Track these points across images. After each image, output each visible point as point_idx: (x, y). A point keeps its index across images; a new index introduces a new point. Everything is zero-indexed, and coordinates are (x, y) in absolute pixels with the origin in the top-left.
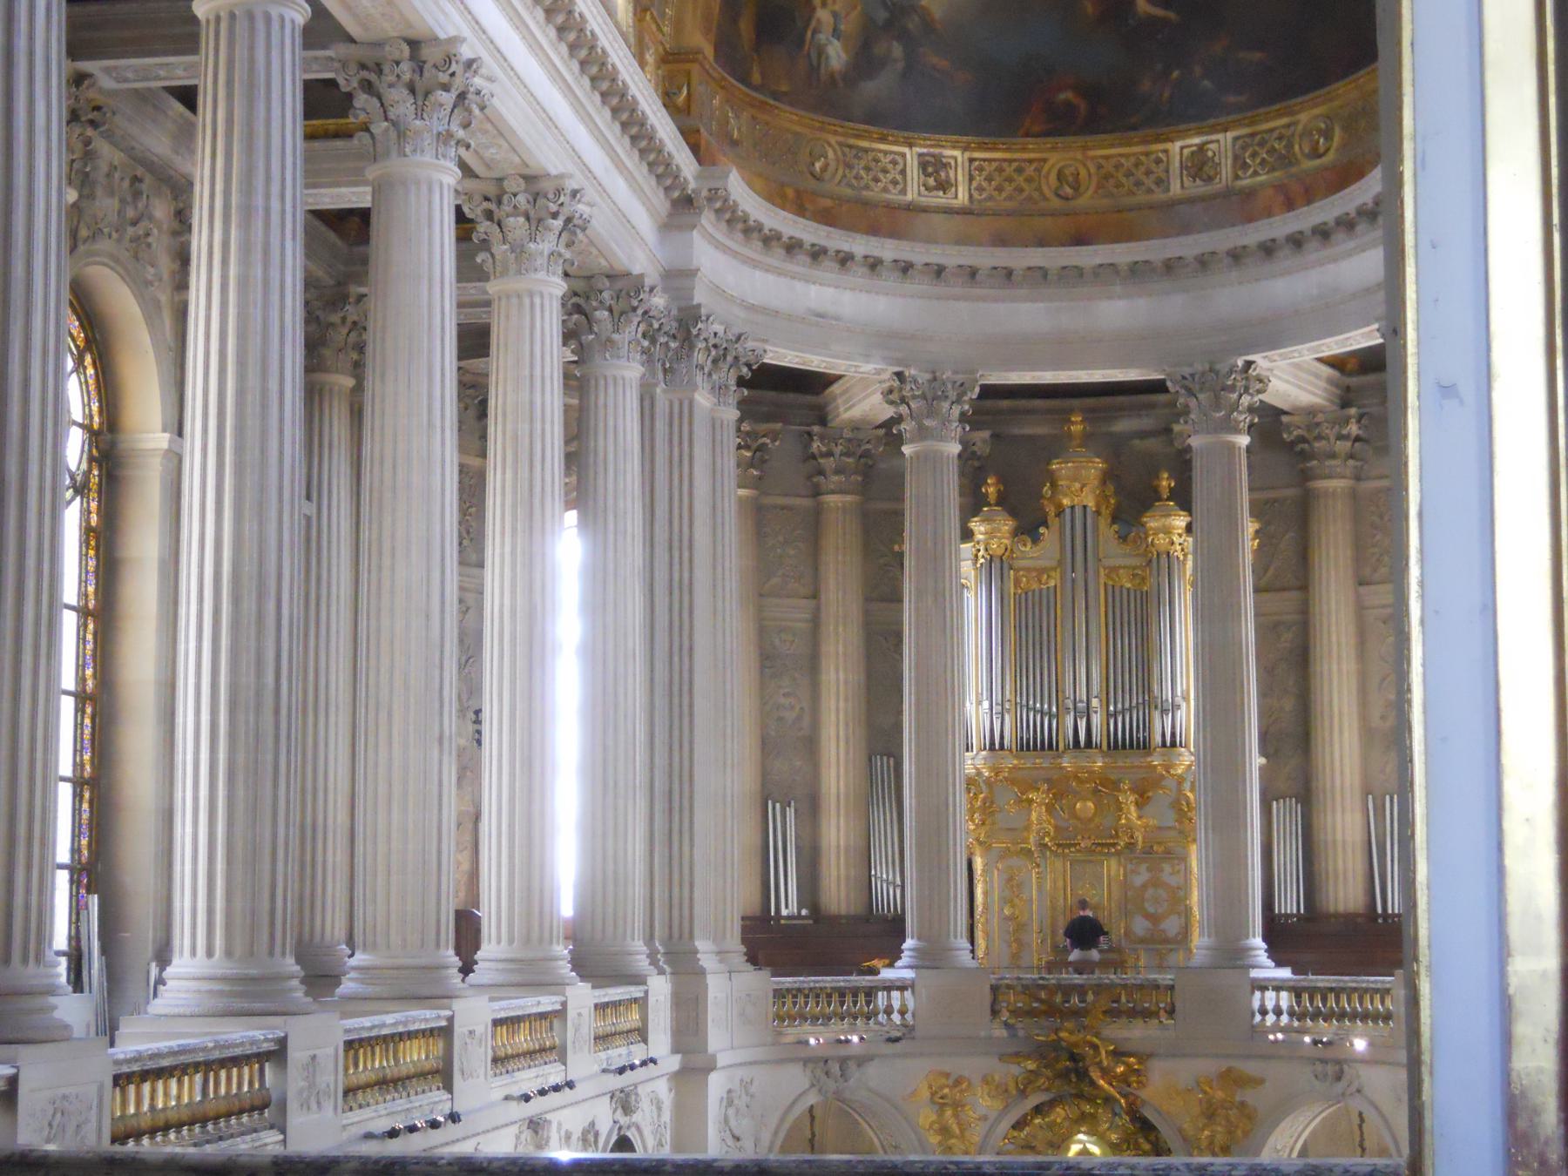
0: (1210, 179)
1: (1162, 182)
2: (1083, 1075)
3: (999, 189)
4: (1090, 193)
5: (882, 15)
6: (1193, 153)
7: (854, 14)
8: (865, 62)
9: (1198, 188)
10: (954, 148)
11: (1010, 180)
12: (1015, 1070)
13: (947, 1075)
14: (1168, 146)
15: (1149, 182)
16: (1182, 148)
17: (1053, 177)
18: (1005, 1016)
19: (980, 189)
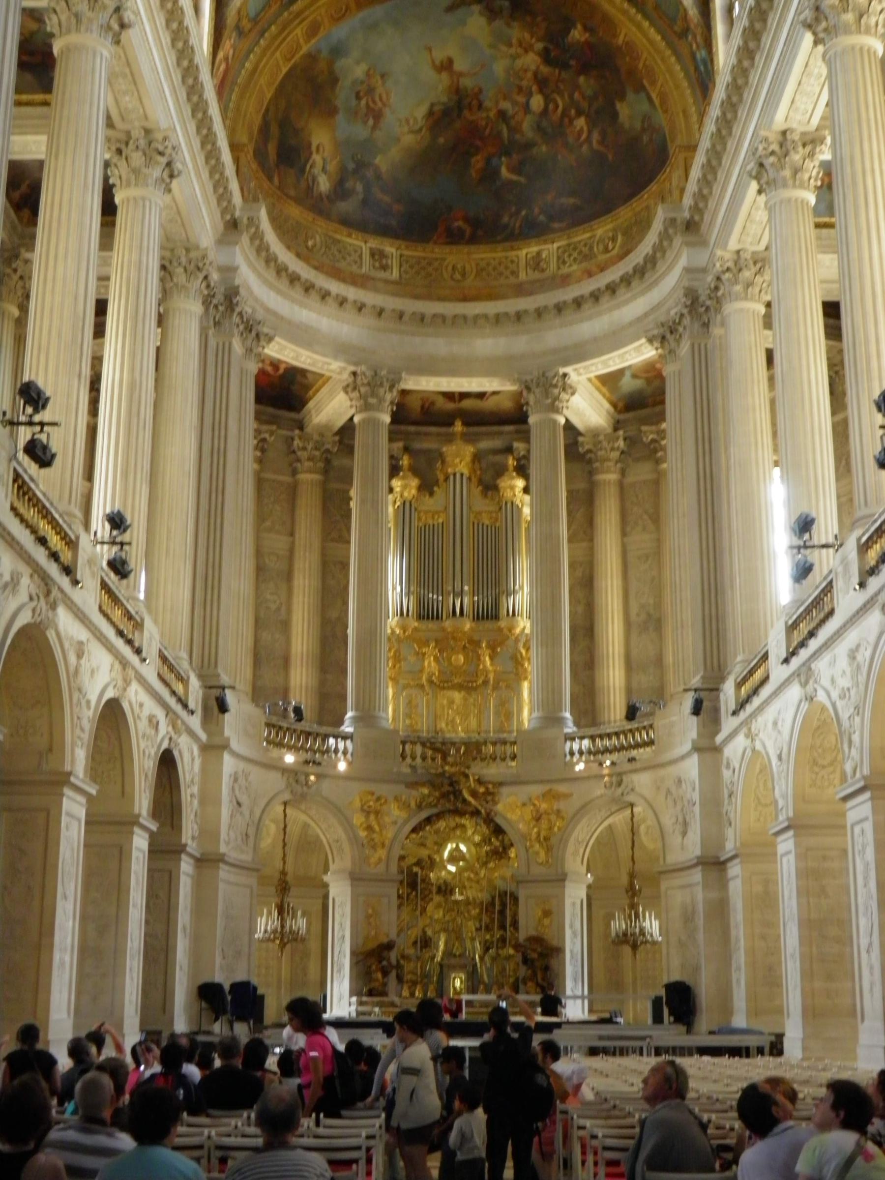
0: (543, 270)
1: (515, 273)
2: (457, 794)
3: (418, 273)
4: (472, 277)
5: (351, 166)
6: (533, 257)
7: (334, 162)
8: (340, 191)
9: (537, 275)
10: (391, 246)
11: (424, 268)
12: (414, 793)
13: (373, 794)
14: (519, 252)
15: (508, 273)
16: (527, 254)
17: (450, 268)
18: (409, 760)
19: (406, 272)
